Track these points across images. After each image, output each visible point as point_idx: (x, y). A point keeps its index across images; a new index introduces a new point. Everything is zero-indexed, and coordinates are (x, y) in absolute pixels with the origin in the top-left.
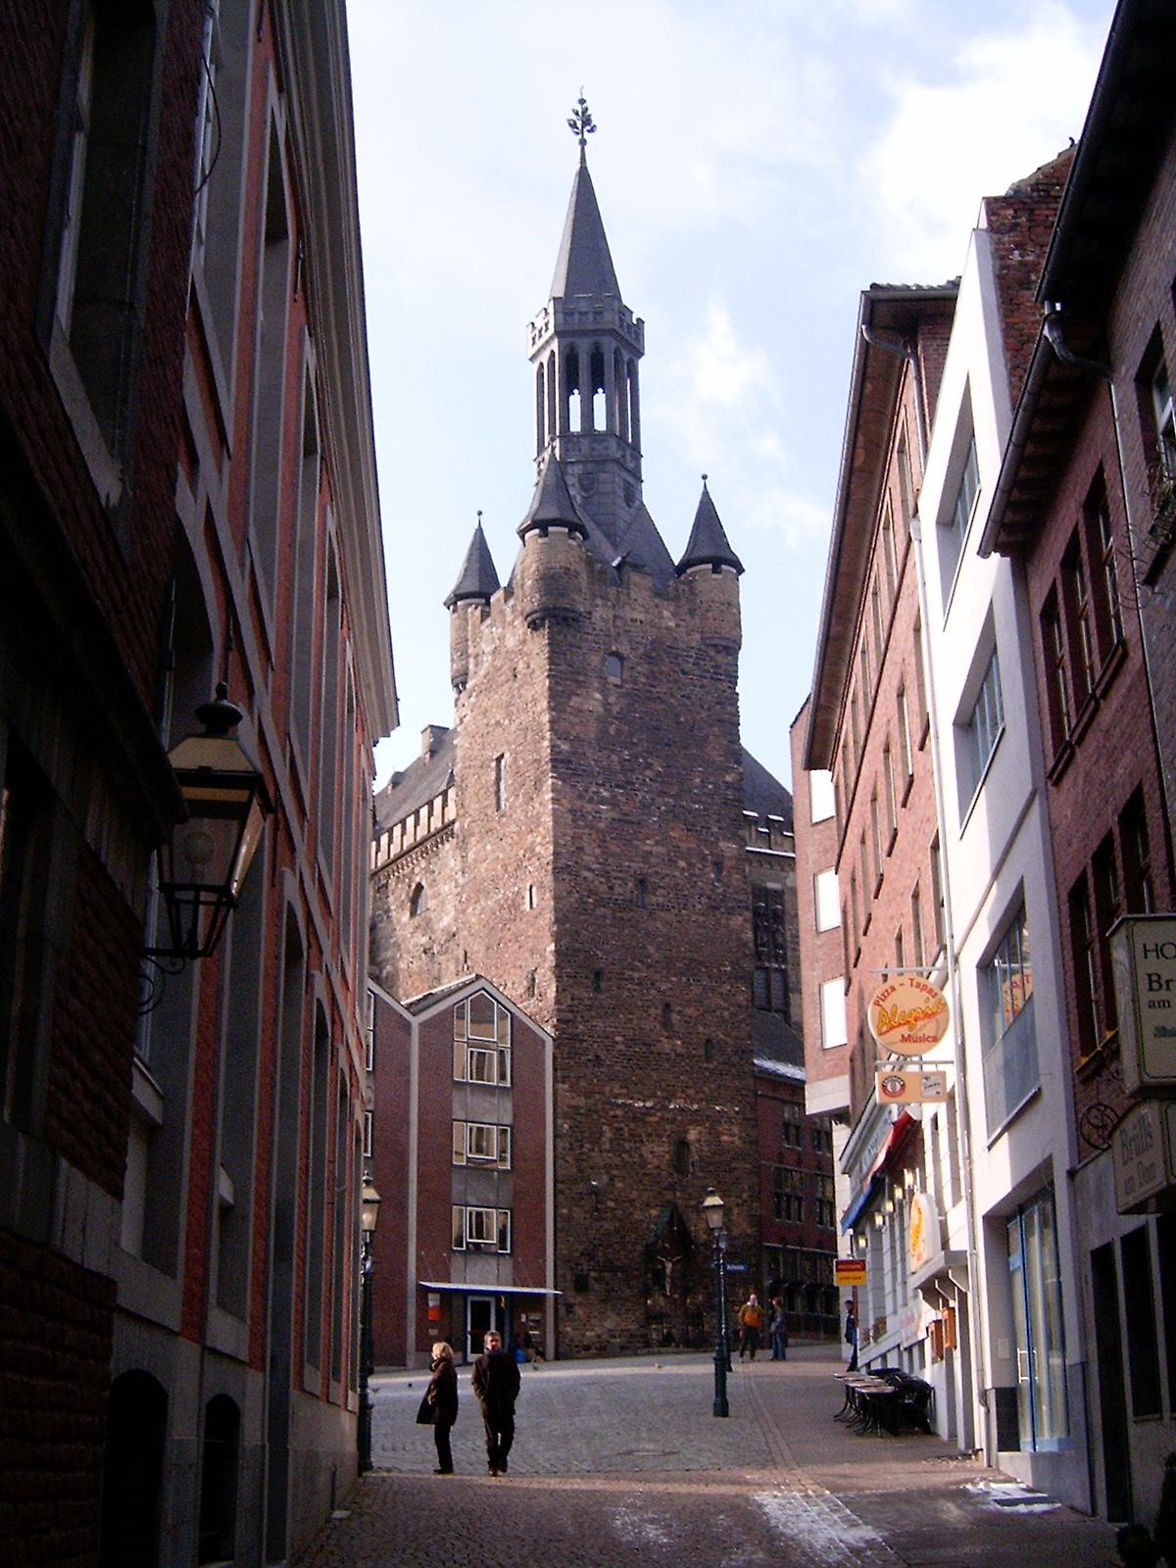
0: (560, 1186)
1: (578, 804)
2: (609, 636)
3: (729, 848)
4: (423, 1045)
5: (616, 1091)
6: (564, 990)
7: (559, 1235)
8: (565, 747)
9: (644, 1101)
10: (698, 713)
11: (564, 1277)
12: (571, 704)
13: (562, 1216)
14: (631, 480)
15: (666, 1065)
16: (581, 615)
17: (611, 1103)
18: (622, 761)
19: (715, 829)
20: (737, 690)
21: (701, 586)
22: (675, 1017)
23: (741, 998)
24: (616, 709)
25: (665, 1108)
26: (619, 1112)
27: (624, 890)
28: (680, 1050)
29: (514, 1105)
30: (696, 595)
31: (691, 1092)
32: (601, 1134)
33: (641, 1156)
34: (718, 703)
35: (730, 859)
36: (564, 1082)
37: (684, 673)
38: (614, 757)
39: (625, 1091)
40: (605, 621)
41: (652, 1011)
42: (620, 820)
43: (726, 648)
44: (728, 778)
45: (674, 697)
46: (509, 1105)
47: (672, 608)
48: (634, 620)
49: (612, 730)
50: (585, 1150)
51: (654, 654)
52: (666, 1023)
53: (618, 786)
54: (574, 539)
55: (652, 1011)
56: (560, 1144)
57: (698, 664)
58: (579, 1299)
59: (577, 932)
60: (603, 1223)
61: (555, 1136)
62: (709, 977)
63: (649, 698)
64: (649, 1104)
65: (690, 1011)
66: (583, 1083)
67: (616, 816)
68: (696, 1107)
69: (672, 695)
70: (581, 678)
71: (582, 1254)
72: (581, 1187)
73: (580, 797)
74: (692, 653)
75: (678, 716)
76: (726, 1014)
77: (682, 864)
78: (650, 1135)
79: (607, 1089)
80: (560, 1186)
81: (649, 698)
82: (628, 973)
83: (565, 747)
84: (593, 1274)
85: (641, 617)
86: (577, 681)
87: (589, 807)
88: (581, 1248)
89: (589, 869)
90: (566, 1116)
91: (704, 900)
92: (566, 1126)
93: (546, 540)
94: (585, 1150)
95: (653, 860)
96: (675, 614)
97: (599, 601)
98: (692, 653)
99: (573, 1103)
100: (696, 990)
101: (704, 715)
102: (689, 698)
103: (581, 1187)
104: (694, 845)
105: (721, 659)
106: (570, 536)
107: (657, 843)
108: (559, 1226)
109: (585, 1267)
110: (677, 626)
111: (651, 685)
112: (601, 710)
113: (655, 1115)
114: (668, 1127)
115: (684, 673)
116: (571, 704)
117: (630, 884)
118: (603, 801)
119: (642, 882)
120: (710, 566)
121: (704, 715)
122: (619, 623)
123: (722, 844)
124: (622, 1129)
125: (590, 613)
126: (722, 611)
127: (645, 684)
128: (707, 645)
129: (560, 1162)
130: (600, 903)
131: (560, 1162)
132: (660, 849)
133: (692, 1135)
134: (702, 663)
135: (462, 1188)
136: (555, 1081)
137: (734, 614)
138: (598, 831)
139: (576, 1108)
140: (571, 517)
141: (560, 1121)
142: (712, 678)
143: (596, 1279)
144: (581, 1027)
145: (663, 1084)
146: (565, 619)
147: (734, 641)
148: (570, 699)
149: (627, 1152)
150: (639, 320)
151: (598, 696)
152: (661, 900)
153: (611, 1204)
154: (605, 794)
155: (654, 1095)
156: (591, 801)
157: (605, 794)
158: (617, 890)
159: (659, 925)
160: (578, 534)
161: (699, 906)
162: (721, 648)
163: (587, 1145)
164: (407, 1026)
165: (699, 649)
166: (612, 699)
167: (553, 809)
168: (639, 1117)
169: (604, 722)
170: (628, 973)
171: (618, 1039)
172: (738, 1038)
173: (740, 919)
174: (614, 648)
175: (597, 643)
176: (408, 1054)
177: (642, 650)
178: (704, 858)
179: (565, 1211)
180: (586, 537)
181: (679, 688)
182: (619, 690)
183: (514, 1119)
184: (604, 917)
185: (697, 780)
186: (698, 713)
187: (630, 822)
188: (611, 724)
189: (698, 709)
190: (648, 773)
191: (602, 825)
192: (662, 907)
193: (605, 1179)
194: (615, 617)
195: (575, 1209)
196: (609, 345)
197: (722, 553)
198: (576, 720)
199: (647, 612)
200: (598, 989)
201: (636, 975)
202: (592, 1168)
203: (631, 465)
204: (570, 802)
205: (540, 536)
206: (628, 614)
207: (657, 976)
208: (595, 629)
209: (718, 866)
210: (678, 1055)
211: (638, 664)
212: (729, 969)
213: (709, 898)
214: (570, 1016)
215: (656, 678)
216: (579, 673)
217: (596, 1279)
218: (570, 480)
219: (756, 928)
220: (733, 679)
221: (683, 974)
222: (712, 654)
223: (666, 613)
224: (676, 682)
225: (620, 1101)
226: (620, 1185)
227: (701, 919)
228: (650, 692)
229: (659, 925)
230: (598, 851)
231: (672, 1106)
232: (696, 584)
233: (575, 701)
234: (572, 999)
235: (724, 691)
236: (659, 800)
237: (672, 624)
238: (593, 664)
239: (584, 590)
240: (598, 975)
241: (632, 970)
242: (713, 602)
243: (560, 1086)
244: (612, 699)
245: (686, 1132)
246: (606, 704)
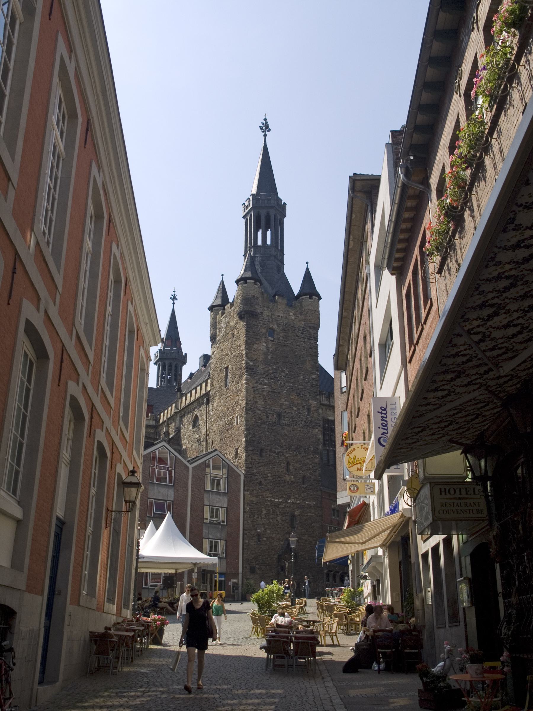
0: (245, 532)
1: (256, 385)
2: (269, 322)
3: (313, 403)
4: (193, 476)
5: (267, 495)
6: (249, 456)
7: (245, 551)
8: (251, 363)
9: (279, 499)
11: (246, 567)
13: (246, 543)
14: (280, 263)
15: (288, 486)
17: (266, 500)
18: (273, 369)
19: (308, 396)
20: (318, 343)
22: (291, 467)
23: (316, 460)
24: (271, 350)
25: (286, 502)
26: (269, 503)
27: (273, 418)
28: (293, 480)
29: (228, 500)
31: (297, 496)
32: (262, 512)
33: (277, 520)
34: (310, 348)
35: (313, 407)
36: (247, 491)
38: (270, 368)
39: (271, 495)
40: (268, 316)
41: (282, 464)
42: (272, 392)
44: (313, 377)
46: (226, 499)
47: (293, 312)
48: (279, 316)
49: (269, 357)
50: (255, 518)
52: (288, 470)
53: (271, 379)
54: (257, 285)
55: (282, 464)
56: (246, 516)
58: (252, 576)
59: (254, 434)
60: (261, 546)
61: (244, 512)
62: (305, 452)
64: (280, 500)
65: (297, 465)
66: (255, 492)
67: (270, 390)
68: (298, 502)
70: (258, 337)
71: (253, 558)
72: (253, 532)
73: (257, 383)
74: (301, 329)
76: (311, 466)
77: (295, 408)
78: (280, 512)
79: (264, 494)
80: (245, 532)
82: (273, 450)
83: (251, 363)
84: (257, 566)
86: (256, 338)
87: (260, 386)
88: (253, 556)
89: (259, 410)
90: (248, 504)
91: (303, 423)
92: (248, 508)
93: (246, 285)
94: (255, 518)
95: (284, 407)
96: (294, 314)
97: (265, 309)
98: (301, 329)
99: (251, 499)
100: (300, 457)
101: (305, 352)
102: (299, 346)
103: (253, 532)
104: (300, 402)
107: (286, 400)
108: (245, 547)
109: (254, 564)
110: (295, 318)
112: (265, 350)
113: (282, 505)
114: (287, 509)
115: (298, 337)
117: (275, 416)
118: (265, 384)
119: (279, 416)
120: (308, 296)
121: (305, 352)
123: (311, 401)
124: (269, 510)
129: (245, 522)
130: (264, 423)
131: (245, 522)
132: (286, 403)
133: (297, 513)
135: (207, 531)
136: (244, 490)
138: (263, 395)
139: (252, 501)
141: (246, 506)
142: (308, 339)
143: (258, 568)
144: (255, 470)
145: (286, 493)
148: (253, 345)
149: (272, 519)
150: (284, 203)
151: (264, 344)
152: (287, 422)
153: (265, 539)
154: (266, 381)
155: (282, 497)
156: (261, 384)
157: (266, 381)
158: (270, 418)
159: (286, 432)
160: (258, 283)
161: (301, 425)
163: (256, 516)
164: (188, 468)
167: (246, 387)
168: (276, 505)
169: (266, 354)
170: (273, 450)
171: (269, 475)
172: (315, 476)
173: (317, 430)
174: (271, 326)
176: (188, 479)
177: (281, 328)
178: (303, 407)
179: (247, 541)
180: (261, 284)
183: (228, 505)
184: (265, 428)
185: (302, 377)
187: (276, 392)
188: (269, 355)
190: (283, 374)
191: (265, 393)
192: (287, 425)
193: (263, 529)
194: (272, 314)
195: (251, 541)
196: (272, 213)
199: (284, 313)
200: (261, 456)
201: (277, 451)
202: (258, 525)
203: (280, 258)
204: (253, 384)
205: (244, 284)
206: (277, 314)
207: (285, 451)
208: (263, 319)
209: (309, 410)
210: (292, 482)
212: (312, 449)
213: (305, 422)
214: (250, 466)
217: (258, 568)
218: (256, 263)
219: (324, 434)
220: (316, 339)
221: (294, 451)
222: (308, 329)
223: (291, 314)
225: (269, 499)
226: (268, 532)
227: (302, 429)
229: (286, 432)
230: (263, 403)
231: (289, 501)
233: (255, 346)
234: (252, 459)
236: (287, 384)
237: (293, 318)
240: (262, 450)
241: (275, 449)
243: (246, 493)
244: (270, 345)
245: (295, 511)
246: (267, 348)
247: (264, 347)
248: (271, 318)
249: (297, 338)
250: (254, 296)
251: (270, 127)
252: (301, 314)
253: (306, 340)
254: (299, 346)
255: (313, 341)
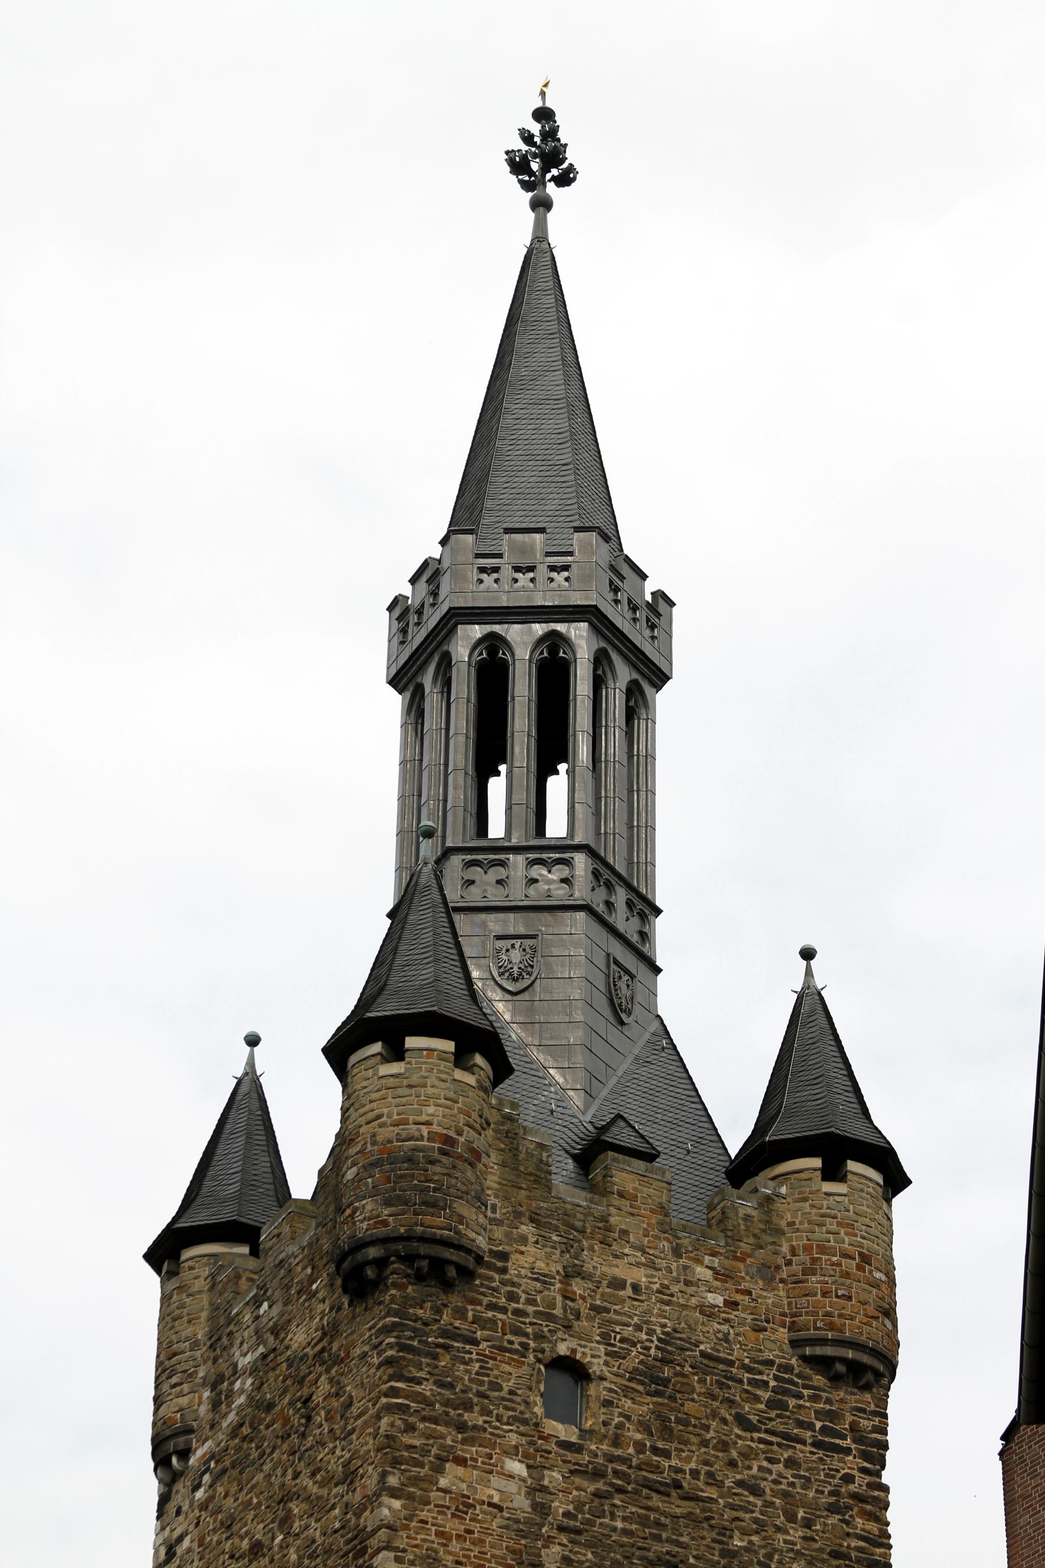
2: (550, 1317)
10: (779, 1529)
12: (443, 1482)
16: (479, 1259)
21: (786, 1213)
24: (560, 1506)
30: (780, 1232)
34: (833, 1509)
37: (742, 1421)
40: (543, 1279)
43: (856, 1370)
45: (719, 1485)
48: (618, 1284)
51: (667, 1372)
54: (470, 1069)
57: (784, 1406)
63: (651, 1487)
69: (712, 1479)
70: (474, 1418)
74: (769, 1376)
75: (725, 1532)
81: (651, 1487)
85: (640, 1276)
86: (462, 1427)
93: (396, 1068)
96: (723, 1276)
97: (527, 1229)
98: (769, 1376)
101: (796, 1534)
102: (756, 1491)
105: (848, 1398)
106: (461, 1059)
110: (732, 1305)
111: (655, 1450)
112: (522, 1503)
116: (443, 1482)
120: (817, 1162)
121: (796, 1534)
122: (578, 1287)
125: (504, 1256)
126: (847, 1275)
127: (640, 1447)
128: (804, 1359)
134: (792, 1402)
137: (875, 1284)
140: (457, 1008)
142: (817, 1444)
146: (438, 1265)
147: (875, 1353)
148: (439, 1469)
151: (517, 1467)
160: (479, 1059)
162: (840, 1368)
165: (787, 1368)
166: (554, 1477)
174: (563, 1349)
175: (518, 1332)
177: (634, 1359)
180: (502, 1069)
181: (732, 1464)
182: (570, 1456)
186: (779, 1529)
188: (549, 1541)
189: (781, 1521)
194: (570, 1274)
197: (855, 1130)
198: (453, 1526)
199: (652, 1265)
205: (386, 1059)
208: (512, 1297)
211: (626, 1391)
215: (667, 1433)
216: (468, 1406)
224: (724, 1446)
228: (657, 1469)
232: (779, 1205)
233: (451, 1477)
235: (848, 1479)
237: (716, 1299)
238: (506, 1386)
239: (492, 1200)
242: (822, 1250)
246: (536, 1489)
247: (512, 1487)
248: (567, 1296)
249: (745, 1441)
250: (448, 1140)
251: (572, 157)
252: (768, 1273)
253: (803, 1452)
254: (756, 1491)
255: (851, 1463)
